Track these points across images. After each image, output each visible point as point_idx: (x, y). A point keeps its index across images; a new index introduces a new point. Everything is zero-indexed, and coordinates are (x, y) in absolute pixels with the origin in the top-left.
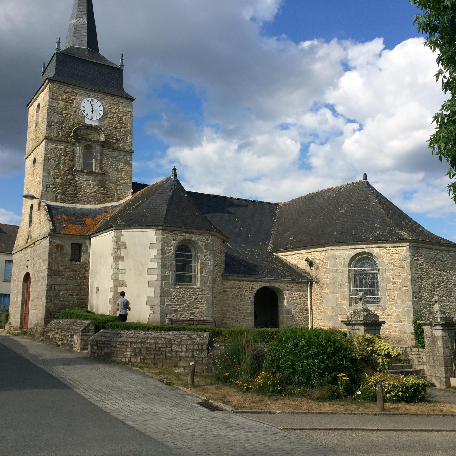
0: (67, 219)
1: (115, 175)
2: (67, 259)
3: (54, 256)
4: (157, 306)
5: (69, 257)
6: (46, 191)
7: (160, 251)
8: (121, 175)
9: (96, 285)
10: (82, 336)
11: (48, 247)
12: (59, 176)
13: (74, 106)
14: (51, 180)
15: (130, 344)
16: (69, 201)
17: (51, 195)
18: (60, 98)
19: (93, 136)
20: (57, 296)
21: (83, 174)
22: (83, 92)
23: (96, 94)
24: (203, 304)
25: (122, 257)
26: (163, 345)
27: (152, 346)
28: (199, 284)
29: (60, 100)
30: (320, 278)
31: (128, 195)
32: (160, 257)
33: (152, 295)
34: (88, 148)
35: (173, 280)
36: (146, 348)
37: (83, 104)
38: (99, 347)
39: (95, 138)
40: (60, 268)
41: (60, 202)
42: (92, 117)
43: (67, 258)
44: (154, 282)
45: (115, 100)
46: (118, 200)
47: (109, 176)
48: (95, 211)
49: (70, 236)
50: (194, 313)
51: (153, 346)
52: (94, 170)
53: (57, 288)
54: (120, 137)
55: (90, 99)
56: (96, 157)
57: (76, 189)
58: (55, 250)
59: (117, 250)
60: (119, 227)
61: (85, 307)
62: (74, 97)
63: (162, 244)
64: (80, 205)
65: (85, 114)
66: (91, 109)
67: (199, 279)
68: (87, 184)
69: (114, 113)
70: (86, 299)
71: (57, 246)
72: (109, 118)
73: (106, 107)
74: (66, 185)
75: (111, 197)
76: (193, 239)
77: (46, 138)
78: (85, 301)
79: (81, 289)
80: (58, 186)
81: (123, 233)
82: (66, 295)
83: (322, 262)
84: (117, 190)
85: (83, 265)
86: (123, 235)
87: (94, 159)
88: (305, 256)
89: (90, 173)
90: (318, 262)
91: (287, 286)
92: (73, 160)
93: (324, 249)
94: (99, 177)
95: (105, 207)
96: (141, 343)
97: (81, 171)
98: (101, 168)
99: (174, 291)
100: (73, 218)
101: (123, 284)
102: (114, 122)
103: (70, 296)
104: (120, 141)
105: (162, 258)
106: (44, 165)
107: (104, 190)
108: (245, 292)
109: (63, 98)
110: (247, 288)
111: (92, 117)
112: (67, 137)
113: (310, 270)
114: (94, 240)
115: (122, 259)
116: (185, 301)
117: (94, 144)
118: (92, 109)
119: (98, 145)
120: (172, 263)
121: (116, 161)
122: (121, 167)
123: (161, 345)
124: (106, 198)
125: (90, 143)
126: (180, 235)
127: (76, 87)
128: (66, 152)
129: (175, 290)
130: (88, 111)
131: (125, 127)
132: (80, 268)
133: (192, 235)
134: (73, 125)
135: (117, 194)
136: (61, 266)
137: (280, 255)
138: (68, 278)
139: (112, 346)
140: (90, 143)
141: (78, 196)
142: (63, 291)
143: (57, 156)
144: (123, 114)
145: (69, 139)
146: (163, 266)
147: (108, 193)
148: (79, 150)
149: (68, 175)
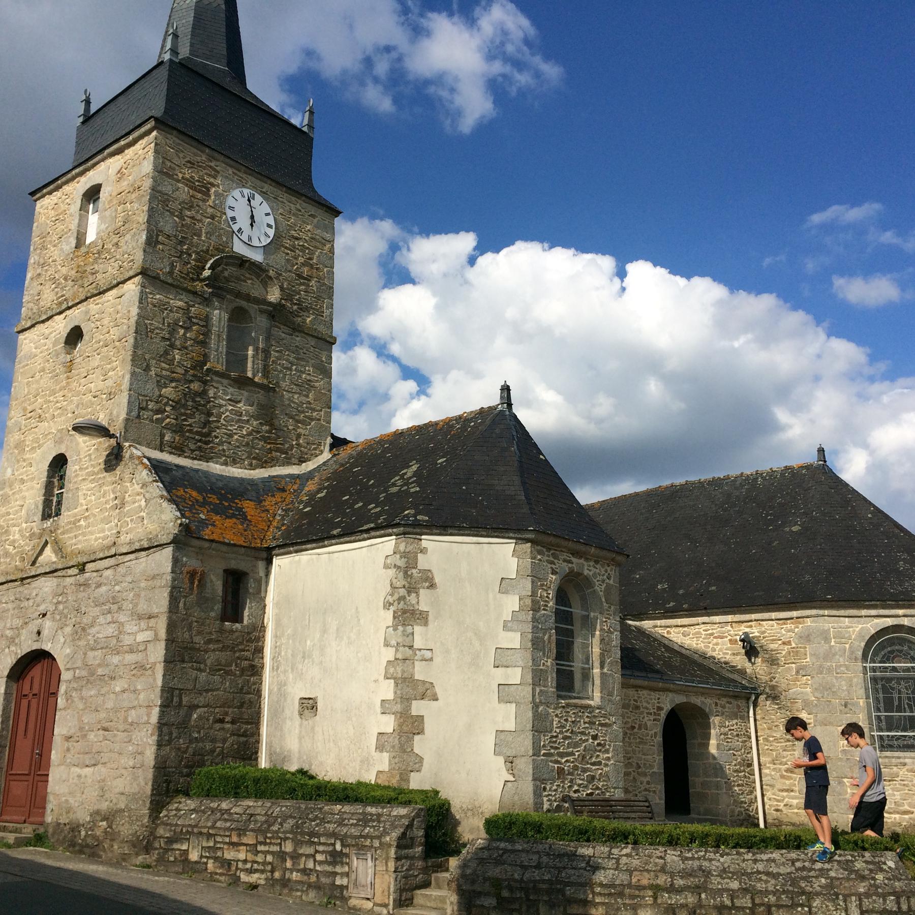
0: (200, 498)
1: (296, 396)
2: (213, 614)
3: (181, 605)
4: (523, 760)
5: (218, 607)
6: (138, 417)
7: (528, 602)
8: (307, 396)
9: (298, 691)
10: (398, 859)
11: (169, 578)
12: (171, 381)
13: (210, 203)
14: (150, 388)
15: (650, 893)
16: (193, 451)
17: (149, 429)
18: (180, 175)
19: (251, 287)
20: (184, 725)
21: (225, 382)
22: (231, 172)
23: (258, 183)
24: (607, 751)
25: (421, 612)
26: (779, 898)
27: (738, 903)
28: (597, 695)
29: (178, 181)
30: (783, 686)
31: (322, 452)
32: (530, 619)
33: (511, 725)
34: (238, 316)
35: (554, 684)
36: (715, 907)
37: (230, 202)
38: (510, 901)
39: (255, 293)
40: (197, 639)
41: (171, 453)
42: (250, 239)
43: (212, 610)
44: (512, 688)
45: (298, 206)
46: (301, 461)
47: (283, 395)
48: (252, 483)
49: (224, 548)
50: (593, 778)
51: (746, 902)
52: (250, 374)
53: (185, 700)
54: (309, 300)
55: (246, 191)
56: (255, 342)
57: (209, 422)
58: (187, 585)
59: (409, 592)
60: (413, 529)
61: (250, 759)
62: (212, 180)
63: (533, 582)
64: (218, 466)
65: (235, 228)
66: (250, 218)
67: (597, 682)
68: (233, 410)
69: (297, 239)
70: (253, 735)
71: (192, 574)
72: (286, 248)
73: (280, 218)
74: (185, 406)
75: (286, 453)
76: (586, 572)
77: (144, 272)
78: (252, 740)
79: (241, 706)
80: (168, 409)
81: (424, 544)
82: (208, 720)
83: (786, 647)
84: (299, 436)
85: (249, 633)
86: (423, 551)
87: (251, 348)
88: (744, 629)
89: (243, 382)
90: (773, 646)
91: (716, 704)
92: (204, 343)
93: (795, 614)
94: (260, 395)
95: (274, 477)
96: (697, 889)
97: (222, 375)
98: (266, 372)
99: (557, 716)
100: (214, 499)
101: (427, 692)
102: (295, 261)
103: (218, 726)
104: (307, 309)
105: (534, 620)
106: (136, 346)
107: (270, 432)
108: (646, 718)
109: (187, 176)
110: (650, 706)
111: (250, 239)
112: (193, 280)
113: (748, 665)
114: (280, 563)
115: (422, 618)
116: (576, 745)
117: (252, 308)
118: (252, 217)
119: (262, 311)
120: (550, 636)
121: (298, 359)
122: (308, 378)
123: (773, 899)
124: (274, 454)
125: (244, 304)
126: (565, 561)
127: (216, 155)
128: (190, 318)
129: (558, 712)
130: (243, 222)
131: (320, 279)
132: (241, 643)
133: (582, 561)
134: (208, 250)
135: (298, 444)
136: (199, 633)
137: (647, 624)
138: (213, 671)
139: (570, 901)
140: (244, 304)
141: (212, 442)
142: (198, 711)
143: (169, 326)
144: (314, 243)
145: (198, 286)
146: (537, 644)
147: (280, 440)
148: (218, 316)
149: (192, 381)
